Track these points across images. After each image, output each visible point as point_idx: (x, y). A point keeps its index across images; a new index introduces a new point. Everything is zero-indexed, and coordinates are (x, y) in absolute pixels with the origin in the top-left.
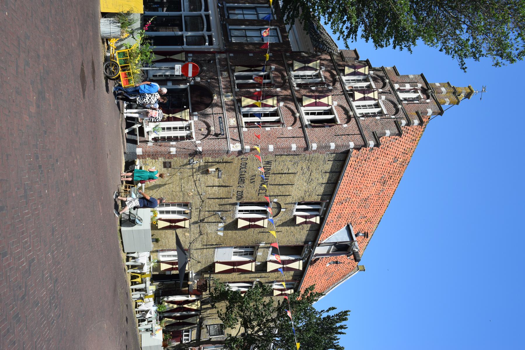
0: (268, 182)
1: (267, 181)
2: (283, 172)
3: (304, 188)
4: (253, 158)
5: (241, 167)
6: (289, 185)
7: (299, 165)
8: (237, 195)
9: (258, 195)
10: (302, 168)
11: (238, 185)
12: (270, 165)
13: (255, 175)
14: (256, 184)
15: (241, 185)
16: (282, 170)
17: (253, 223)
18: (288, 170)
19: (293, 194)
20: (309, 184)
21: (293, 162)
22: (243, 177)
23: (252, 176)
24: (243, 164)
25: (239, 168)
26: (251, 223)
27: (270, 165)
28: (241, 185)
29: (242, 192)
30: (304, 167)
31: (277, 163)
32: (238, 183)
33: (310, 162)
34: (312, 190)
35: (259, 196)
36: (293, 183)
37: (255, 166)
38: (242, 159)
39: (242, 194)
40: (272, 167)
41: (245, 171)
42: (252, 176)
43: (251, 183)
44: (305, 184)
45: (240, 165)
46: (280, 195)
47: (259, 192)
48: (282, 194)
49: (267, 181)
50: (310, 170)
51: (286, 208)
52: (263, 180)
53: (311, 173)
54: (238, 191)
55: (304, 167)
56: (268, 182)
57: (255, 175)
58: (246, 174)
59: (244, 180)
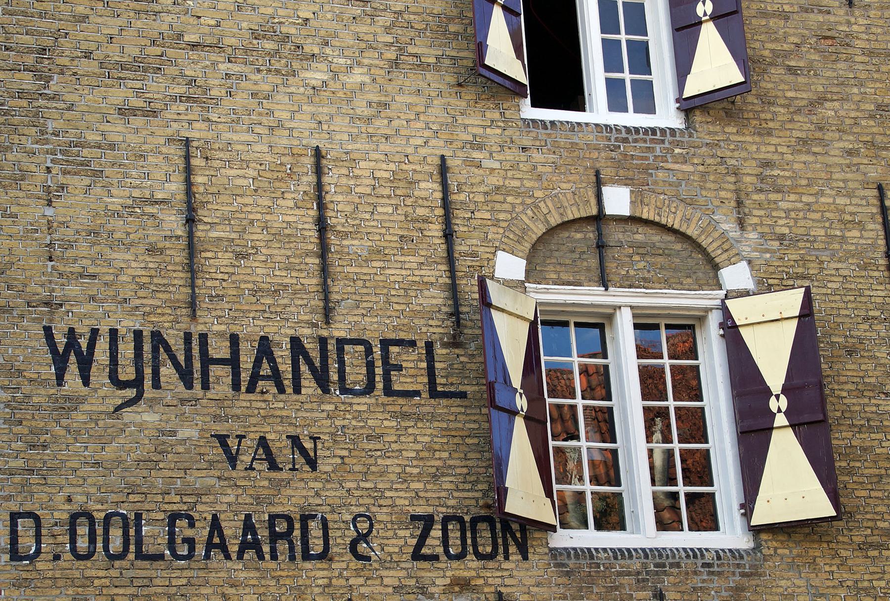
0: (296, 343)
1: (283, 355)
2: (183, 243)
3: (358, 76)
4: (12, 473)
5: (122, 556)
6: (319, 186)
7: (92, 137)
8: (461, 556)
9: (463, 395)
10: (125, 112)
11: (343, 561)
12: (102, 345)
13: (222, 440)
14: (323, 428)
15: (341, 539)
16: (152, 250)
17: (778, 404)
18: (149, 209)
19: (438, 147)
20: (312, 48)
21: (61, 179)
22: (248, 526)
23: (233, 460)
24: (82, 544)
25: (145, 569)
26: (781, 420)
27: (102, 345)
28: (341, 539)
29: (428, 521)
30: (118, 95)
31: (73, 290)
32: (324, 555)
33: (65, 61)
34: (385, 19)
35: (468, 389)
36: (308, 161)
37: (109, 453)
38: (15, 554)
39: (446, 520)
40: (127, 324)
41: (174, 517)
42: (233, 460)
43: (312, 464)
44: (316, 75)
45: (95, 569)
46: (448, 235)
47: (417, 393)
48: (435, 230)
49: (283, 355)
50: (158, 50)
51: (599, 184)
52: (276, 376)
53: (194, 46)
54: (417, 555)
55: (118, 95)
56: (296, 343)
57: (222, 440)
58: (203, 512)
59: (273, 517)
